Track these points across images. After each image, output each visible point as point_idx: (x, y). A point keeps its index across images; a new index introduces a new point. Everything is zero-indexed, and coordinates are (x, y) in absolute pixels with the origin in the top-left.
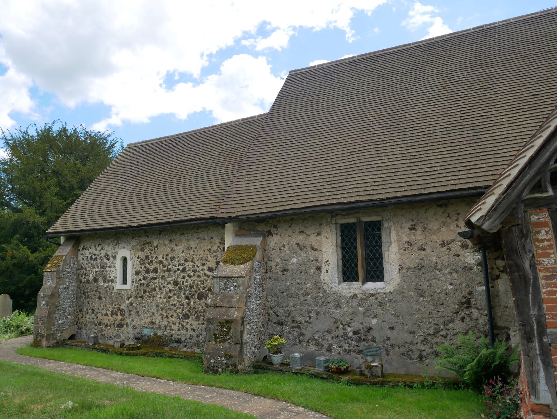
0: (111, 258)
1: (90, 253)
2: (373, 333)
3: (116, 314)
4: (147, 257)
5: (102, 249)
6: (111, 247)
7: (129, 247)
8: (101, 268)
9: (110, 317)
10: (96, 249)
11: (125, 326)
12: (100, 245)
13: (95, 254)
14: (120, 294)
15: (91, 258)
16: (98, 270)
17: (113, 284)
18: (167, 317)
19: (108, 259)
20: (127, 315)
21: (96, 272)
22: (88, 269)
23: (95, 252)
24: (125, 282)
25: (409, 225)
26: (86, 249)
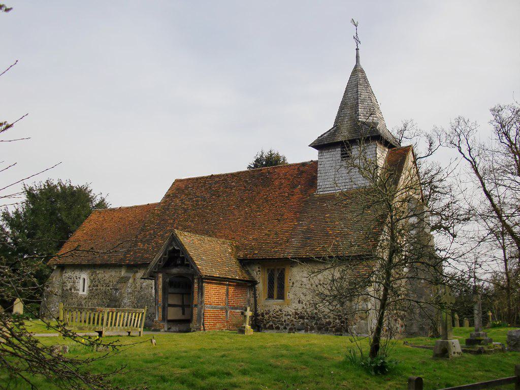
4: (94, 279)
26: (67, 273)
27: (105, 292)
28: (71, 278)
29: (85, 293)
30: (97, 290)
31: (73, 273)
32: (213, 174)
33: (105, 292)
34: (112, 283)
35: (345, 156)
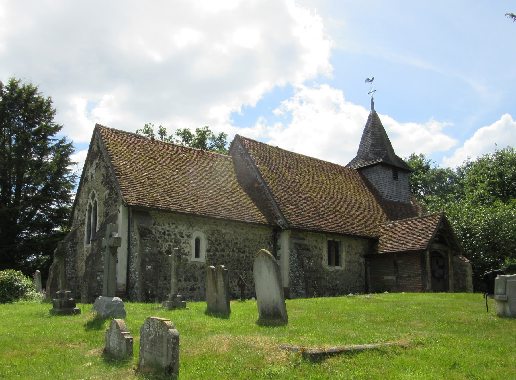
0: (185, 236)
1: (163, 229)
3: (190, 281)
4: (216, 240)
5: (176, 227)
6: (185, 227)
7: (202, 230)
9: (183, 283)
10: (170, 227)
11: (197, 289)
12: (174, 224)
13: (168, 231)
14: (194, 265)
15: (164, 233)
16: (172, 244)
17: (187, 257)
18: (231, 282)
19: (183, 237)
20: (199, 281)
21: (170, 245)
22: (160, 242)
23: (168, 229)
24: (197, 255)
28: (169, 235)
29: (203, 258)
30: (223, 256)
33: (238, 260)
34: (247, 249)
35: (395, 177)
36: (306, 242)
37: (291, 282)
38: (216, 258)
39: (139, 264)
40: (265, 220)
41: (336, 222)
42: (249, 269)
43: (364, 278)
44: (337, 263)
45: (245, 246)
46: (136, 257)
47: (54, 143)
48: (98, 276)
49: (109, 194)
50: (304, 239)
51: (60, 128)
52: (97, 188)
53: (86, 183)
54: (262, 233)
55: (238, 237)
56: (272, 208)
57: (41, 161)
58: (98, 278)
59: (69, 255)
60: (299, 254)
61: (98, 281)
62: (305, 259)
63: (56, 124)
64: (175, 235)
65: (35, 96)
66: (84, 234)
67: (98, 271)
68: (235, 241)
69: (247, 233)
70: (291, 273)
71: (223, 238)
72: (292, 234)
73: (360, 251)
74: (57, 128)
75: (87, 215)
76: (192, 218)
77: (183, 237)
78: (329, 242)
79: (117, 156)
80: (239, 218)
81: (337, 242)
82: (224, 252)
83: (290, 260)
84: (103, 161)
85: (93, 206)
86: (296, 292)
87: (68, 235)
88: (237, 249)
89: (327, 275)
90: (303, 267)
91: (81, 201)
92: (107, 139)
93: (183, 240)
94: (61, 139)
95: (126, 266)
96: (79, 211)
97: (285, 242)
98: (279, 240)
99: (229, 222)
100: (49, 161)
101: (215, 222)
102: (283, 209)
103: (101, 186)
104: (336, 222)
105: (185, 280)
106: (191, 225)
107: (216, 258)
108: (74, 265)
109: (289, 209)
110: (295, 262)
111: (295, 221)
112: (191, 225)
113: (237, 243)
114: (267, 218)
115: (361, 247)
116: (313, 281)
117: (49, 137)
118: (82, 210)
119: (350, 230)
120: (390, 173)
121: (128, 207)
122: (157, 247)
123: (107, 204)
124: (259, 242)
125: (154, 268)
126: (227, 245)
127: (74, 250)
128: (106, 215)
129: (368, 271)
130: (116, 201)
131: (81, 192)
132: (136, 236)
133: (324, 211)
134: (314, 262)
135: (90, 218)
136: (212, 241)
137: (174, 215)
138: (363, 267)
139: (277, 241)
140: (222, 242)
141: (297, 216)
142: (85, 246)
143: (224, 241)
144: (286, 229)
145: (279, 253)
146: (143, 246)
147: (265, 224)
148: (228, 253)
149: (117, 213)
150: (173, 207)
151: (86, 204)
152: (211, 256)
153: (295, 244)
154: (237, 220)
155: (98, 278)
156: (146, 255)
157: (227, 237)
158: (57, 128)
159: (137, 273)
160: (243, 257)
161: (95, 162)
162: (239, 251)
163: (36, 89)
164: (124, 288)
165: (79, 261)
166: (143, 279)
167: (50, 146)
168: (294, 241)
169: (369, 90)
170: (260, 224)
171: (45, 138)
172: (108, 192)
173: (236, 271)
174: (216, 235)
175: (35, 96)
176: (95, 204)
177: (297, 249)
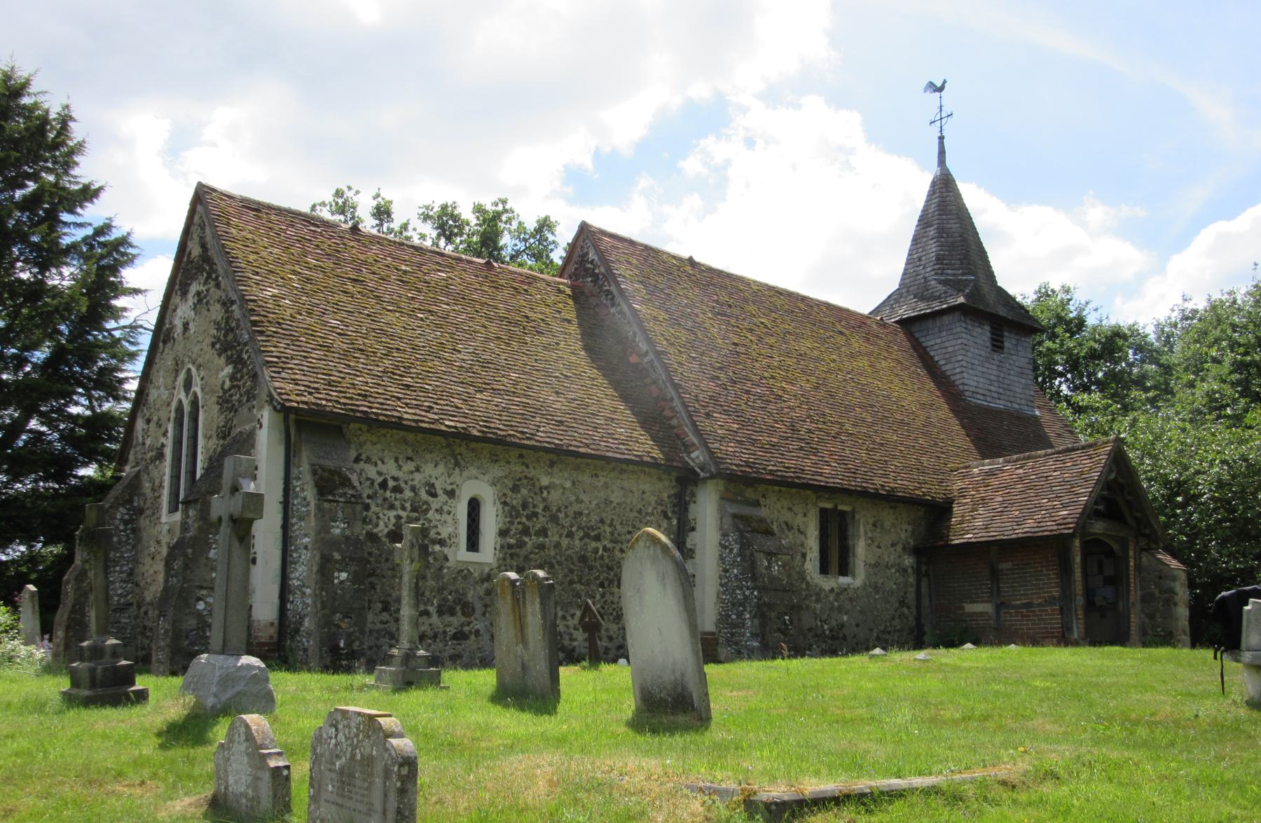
0: (439, 492)
1: (380, 473)
2: (845, 631)
3: (452, 612)
5: (418, 469)
7: (486, 478)
8: (414, 509)
9: (435, 619)
10: (400, 467)
11: (473, 637)
12: (411, 459)
14: (463, 573)
15: (384, 485)
16: (404, 514)
17: (446, 550)
18: (564, 617)
19: (434, 495)
21: (399, 517)
22: (374, 508)
23: (396, 473)
24: (473, 545)
25: (871, 520)
27: (583, 559)
28: (398, 490)
29: (488, 552)
30: (542, 547)
31: (410, 466)
32: (697, 259)
33: (583, 559)
34: (608, 529)
35: (997, 345)
36: (763, 512)
37: (723, 619)
38: (523, 552)
39: (315, 569)
40: (657, 453)
41: (842, 461)
42: (611, 582)
43: (914, 609)
44: (844, 570)
45: (602, 521)
46: (306, 548)
47: (79, 235)
48: (199, 599)
49: (233, 378)
50: (757, 504)
51: (96, 193)
52: (200, 360)
53: (169, 345)
54: (647, 487)
55: (582, 497)
56: (674, 422)
57: (42, 282)
58: (201, 606)
59: (119, 542)
60: (745, 545)
61: (199, 615)
62: (759, 556)
63: (85, 181)
64: (413, 489)
65: (26, 101)
66: (161, 486)
67: (201, 588)
68: (576, 507)
69: (606, 486)
70: (724, 593)
71: (544, 500)
72: (727, 490)
73: (903, 536)
74: (89, 194)
75: (170, 434)
76: (459, 445)
77: (434, 495)
78: (823, 512)
79: (257, 274)
80: (587, 446)
81: (843, 513)
82: (546, 536)
83: (722, 558)
84: (218, 286)
85: (187, 408)
86: (736, 643)
87: (119, 488)
88: (579, 528)
89: (818, 601)
90: (754, 578)
91: (153, 394)
92: (228, 224)
93: (435, 504)
94: (98, 223)
95: (278, 572)
96: (148, 421)
97: (708, 510)
98: (692, 506)
99: (559, 455)
100: (66, 283)
101: (521, 456)
102: (704, 424)
103: (210, 354)
104: (842, 461)
105: (440, 613)
106: (457, 464)
107: (523, 552)
108: (132, 570)
109: (719, 425)
110: (733, 565)
111: (735, 455)
112: (457, 464)
113: (581, 514)
114: (661, 447)
115: (905, 526)
116: (780, 616)
117: (65, 217)
118: (155, 418)
119: (878, 481)
120: (983, 334)
121: (284, 411)
122: (364, 521)
123: (225, 402)
124: (640, 512)
125: (355, 578)
126: (554, 519)
127: (134, 530)
128: (224, 433)
129: (924, 589)
130: (250, 395)
131: (154, 370)
132: (307, 491)
133: (810, 431)
134: (783, 566)
135: (178, 443)
136: (513, 507)
137: (410, 437)
138: (912, 580)
139: (686, 510)
140: (540, 511)
141: (740, 442)
142: (164, 519)
143: (546, 508)
144: (712, 477)
145: (692, 539)
146: (325, 518)
147: (655, 464)
148: (556, 538)
149: (254, 429)
150: (408, 414)
151: (169, 405)
152: (510, 546)
153: (735, 516)
154: (582, 450)
155: (201, 606)
156: (334, 544)
157: (555, 497)
158: (89, 194)
159: (308, 591)
160: (596, 551)
161: (194, 288)
162: (587, 535)
163: (26, 84)
164: (273, 631)
165: (148, 561)
166: (323, 608)
167: (66, 241)
168: (732, 509)
169: (933, 113)
170: (641, 463)
171: (52, 220)
172: (229, 370)
173: (578, 586)
174: (524, 491)
175: (26, 101)
176: (195, 403)
177: (738, 530)
